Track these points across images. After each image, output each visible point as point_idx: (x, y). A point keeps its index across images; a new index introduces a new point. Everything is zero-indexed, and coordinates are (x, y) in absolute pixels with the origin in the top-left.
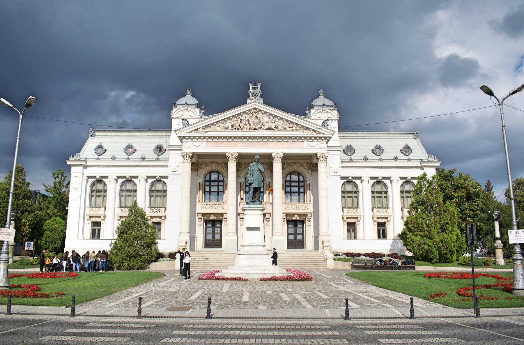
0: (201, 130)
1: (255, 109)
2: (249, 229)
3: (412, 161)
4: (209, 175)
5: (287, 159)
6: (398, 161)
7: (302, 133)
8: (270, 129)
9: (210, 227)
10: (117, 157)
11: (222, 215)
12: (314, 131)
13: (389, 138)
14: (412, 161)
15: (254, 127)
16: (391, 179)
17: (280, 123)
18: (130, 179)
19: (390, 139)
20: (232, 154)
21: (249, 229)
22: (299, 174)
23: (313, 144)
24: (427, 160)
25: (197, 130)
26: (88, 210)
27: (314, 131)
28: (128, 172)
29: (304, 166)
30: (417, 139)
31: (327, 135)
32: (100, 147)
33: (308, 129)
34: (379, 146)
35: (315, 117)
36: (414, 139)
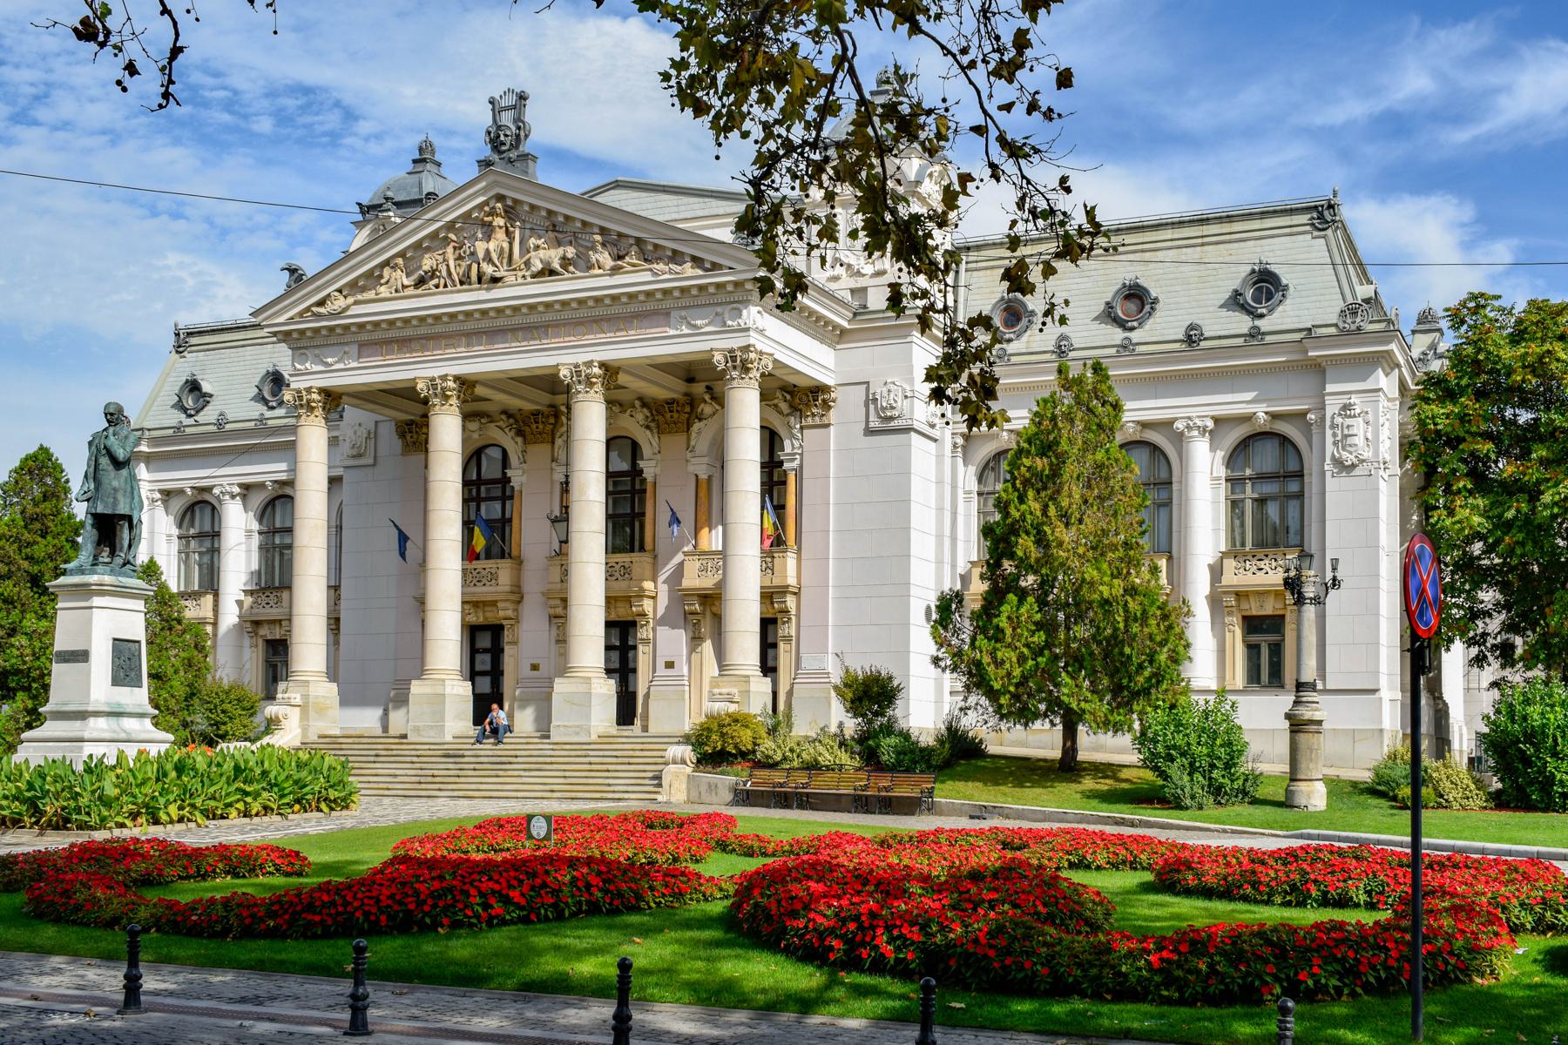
3: (1268, 339)
4: (474, 462)
6: (1202, 343)
7: (647, 277)
9: (485, 651)
10: (230, 417)
13: (1199, 241)
14: (1268, 339)
16: (1180, 425)
18: (200, 498)
19: (1203, 245)
24: (1333, 330)
29: (776, 401)
30: (1329, 232)
32: (193, 386)
34: (1138, 286)
36: (1316, 233)
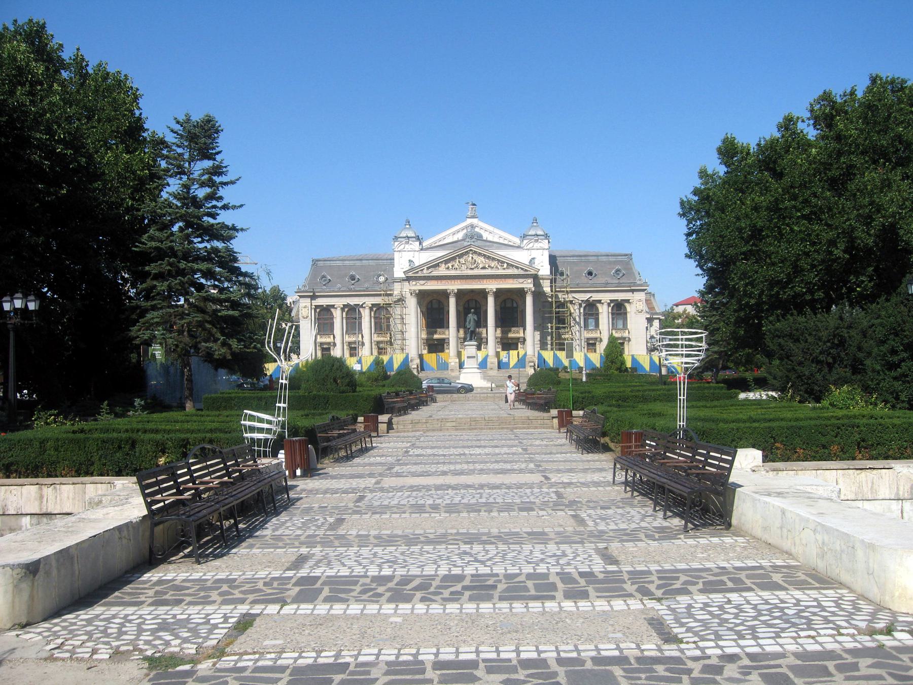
0: (425, 271)
1: (471, 250)
2: (468, 357)
5: (499, 293)
8: (484, 268)
11: (443, 340)
12: (522, 269)
15: (470, 266)
17: (493, 264)
20: (453, 290)
21: (468, 357)
22: (512, 300)
23: (521, 280)
25: (422, 270)
26: (319, 336)
27: (522, 269)
28: (353, 301)
31: (533, 272)
33: (517, 268)
35: (528, 247)
